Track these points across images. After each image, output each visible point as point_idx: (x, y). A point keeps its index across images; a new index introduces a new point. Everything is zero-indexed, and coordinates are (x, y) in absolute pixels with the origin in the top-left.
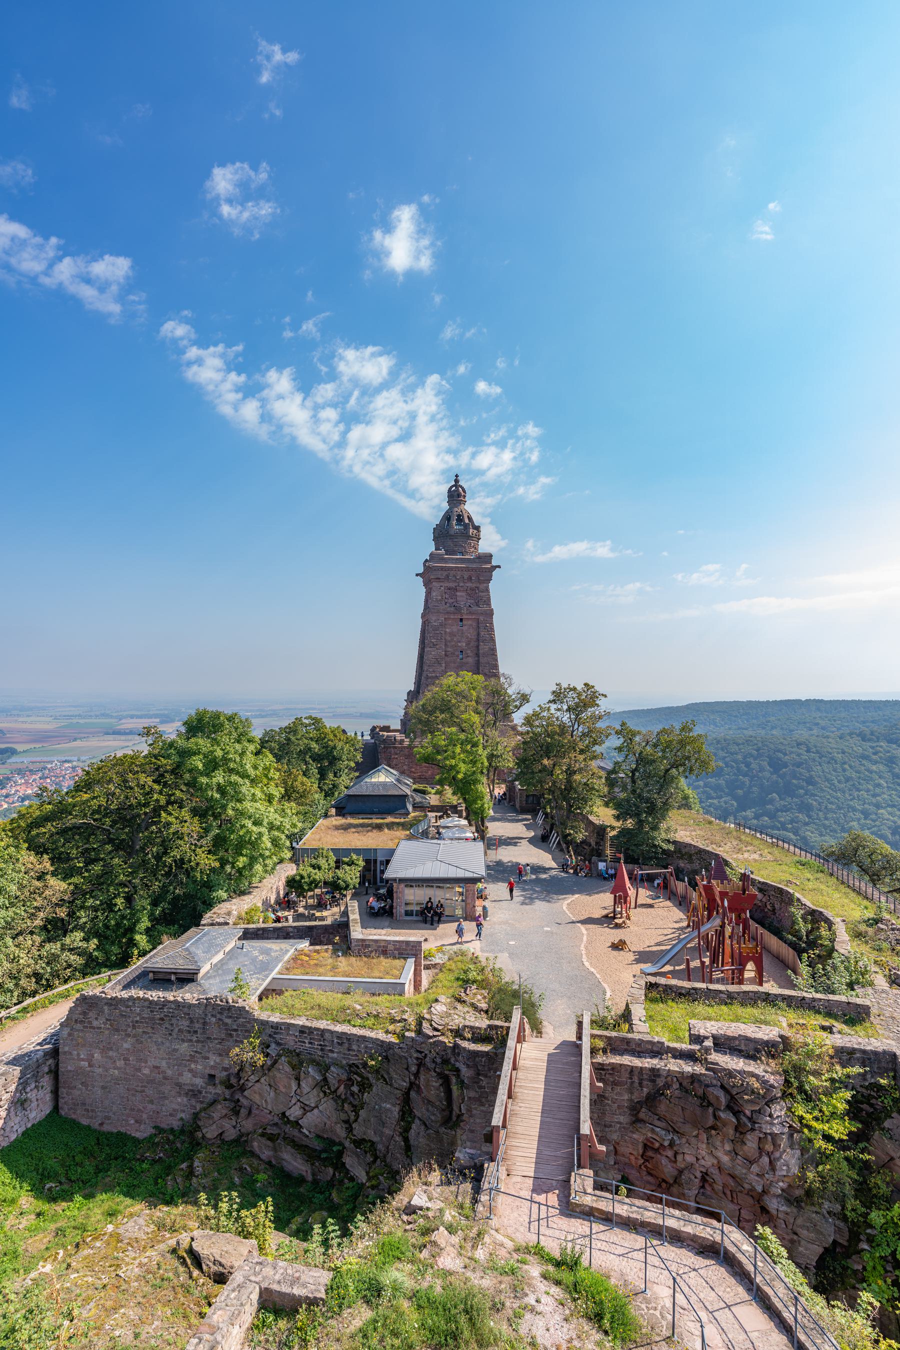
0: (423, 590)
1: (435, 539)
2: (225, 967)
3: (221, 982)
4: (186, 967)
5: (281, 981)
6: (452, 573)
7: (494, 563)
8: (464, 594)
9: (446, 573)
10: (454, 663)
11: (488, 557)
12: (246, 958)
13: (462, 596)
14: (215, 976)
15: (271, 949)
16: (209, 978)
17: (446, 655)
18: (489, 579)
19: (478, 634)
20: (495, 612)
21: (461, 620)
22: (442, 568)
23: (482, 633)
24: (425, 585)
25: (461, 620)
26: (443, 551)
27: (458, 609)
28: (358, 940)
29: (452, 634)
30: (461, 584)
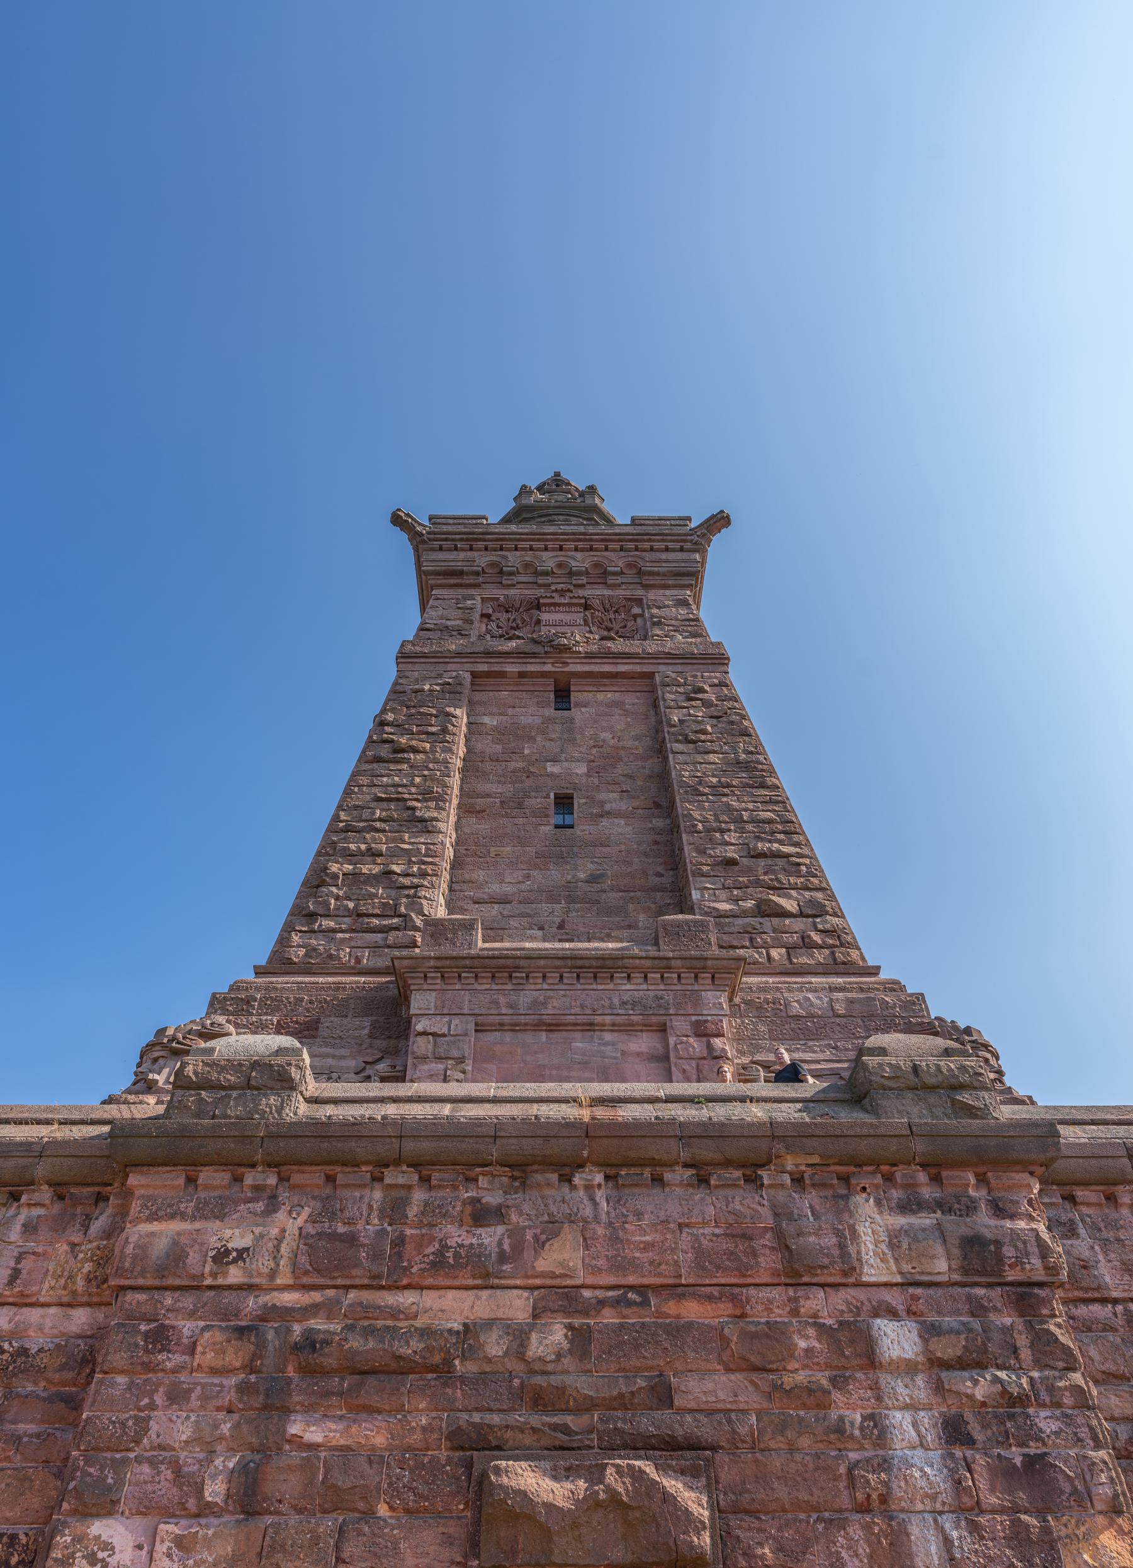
6: (513, 559)
9: (493, 557)
20: (730, 651)
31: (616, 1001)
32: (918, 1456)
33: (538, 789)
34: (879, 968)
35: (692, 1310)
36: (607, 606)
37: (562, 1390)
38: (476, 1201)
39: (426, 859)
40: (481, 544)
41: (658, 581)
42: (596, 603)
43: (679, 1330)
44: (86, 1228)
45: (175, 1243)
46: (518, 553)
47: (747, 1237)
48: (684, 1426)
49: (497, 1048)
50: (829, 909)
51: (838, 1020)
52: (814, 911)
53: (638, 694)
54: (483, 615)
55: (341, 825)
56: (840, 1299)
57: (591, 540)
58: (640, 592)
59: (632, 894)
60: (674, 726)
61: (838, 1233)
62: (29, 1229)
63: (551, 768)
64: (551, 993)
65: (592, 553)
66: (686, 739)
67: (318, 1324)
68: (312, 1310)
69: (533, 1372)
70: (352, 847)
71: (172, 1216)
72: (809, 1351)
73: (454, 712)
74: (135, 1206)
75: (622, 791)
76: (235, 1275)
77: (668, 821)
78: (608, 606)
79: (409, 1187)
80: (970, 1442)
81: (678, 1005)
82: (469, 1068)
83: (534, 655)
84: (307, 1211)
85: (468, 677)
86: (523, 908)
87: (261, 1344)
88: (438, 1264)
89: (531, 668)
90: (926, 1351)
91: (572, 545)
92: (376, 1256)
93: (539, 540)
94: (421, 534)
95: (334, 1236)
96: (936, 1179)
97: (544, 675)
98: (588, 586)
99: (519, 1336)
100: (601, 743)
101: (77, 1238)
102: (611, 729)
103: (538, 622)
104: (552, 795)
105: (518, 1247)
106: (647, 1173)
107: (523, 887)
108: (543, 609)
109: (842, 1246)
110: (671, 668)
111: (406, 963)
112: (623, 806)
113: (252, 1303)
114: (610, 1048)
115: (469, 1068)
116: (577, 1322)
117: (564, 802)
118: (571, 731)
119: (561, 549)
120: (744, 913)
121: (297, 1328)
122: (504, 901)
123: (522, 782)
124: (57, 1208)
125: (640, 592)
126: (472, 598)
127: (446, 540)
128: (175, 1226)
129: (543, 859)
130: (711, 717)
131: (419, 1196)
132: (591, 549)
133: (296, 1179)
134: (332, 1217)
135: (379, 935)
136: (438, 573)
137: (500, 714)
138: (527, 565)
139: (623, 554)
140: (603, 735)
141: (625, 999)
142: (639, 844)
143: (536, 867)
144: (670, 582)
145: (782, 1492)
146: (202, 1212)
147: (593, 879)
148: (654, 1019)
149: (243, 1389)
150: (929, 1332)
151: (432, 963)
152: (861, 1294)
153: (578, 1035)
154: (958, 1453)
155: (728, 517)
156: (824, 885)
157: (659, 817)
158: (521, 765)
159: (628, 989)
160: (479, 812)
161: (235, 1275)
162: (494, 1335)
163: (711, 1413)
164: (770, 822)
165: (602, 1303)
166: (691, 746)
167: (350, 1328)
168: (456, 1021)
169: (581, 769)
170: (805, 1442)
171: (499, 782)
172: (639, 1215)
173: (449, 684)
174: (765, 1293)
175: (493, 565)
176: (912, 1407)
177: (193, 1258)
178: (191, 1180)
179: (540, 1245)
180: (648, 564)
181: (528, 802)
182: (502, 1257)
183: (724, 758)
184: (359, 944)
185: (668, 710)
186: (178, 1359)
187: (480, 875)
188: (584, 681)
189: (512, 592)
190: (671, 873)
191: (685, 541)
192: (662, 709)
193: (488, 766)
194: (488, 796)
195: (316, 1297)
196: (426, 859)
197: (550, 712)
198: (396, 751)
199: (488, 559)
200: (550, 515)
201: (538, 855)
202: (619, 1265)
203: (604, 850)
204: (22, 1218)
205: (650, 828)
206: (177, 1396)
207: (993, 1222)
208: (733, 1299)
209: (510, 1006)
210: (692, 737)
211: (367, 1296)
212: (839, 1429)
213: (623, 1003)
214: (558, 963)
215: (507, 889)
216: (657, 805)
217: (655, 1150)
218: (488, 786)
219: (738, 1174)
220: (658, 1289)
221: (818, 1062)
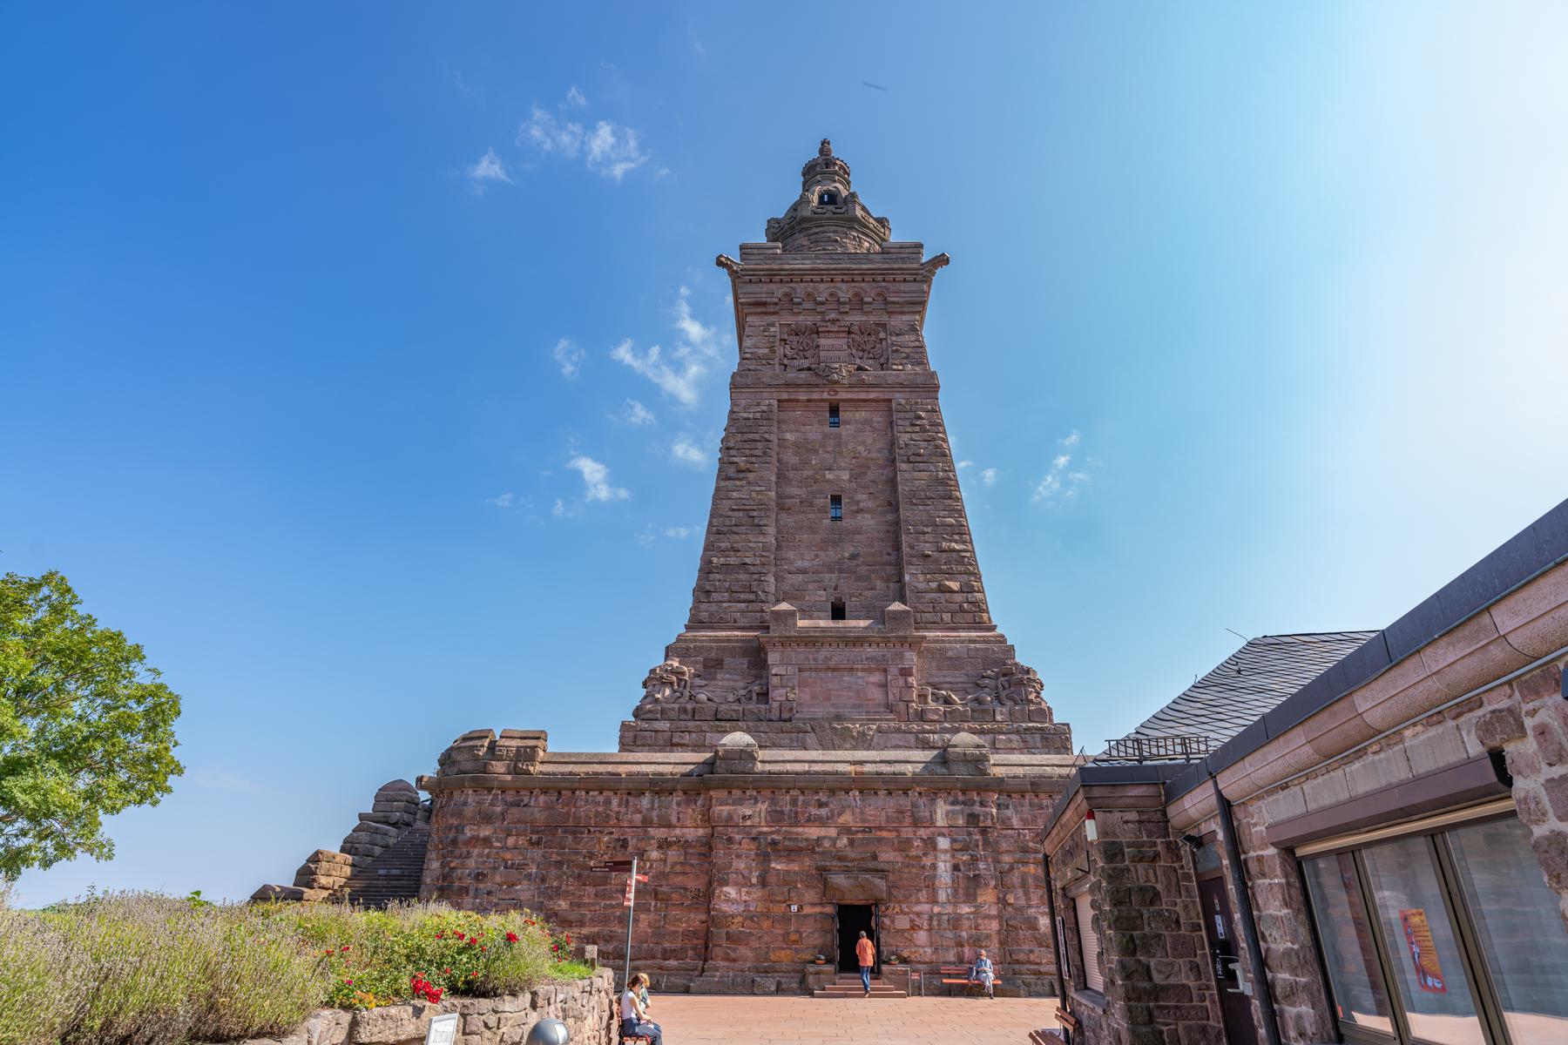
6: (800, 290)
8: (842, 342)
9: (785, 289)
10: (813, 531)
13: (831, 349)
18: (919, 305)
19: (892, 444)
20: (942, 381)
21: (834, 410)
23: (904, 438)
25: (834, 410)
27: (821, 376)
29: (803, 447)
31: (864, 657)
32: (944, 875)
33: (821, 492)
34: (996, 626)
35: (884, 834)
36: (863, 330)
37: (846, 856)
38: (819, 800)
39: (764, 554)
40: (777, 278)
41: (897, 308)
42: (855, 329)
43: (880, 840)
44: (696, 804)
45: (729, 813)
46: (803, 285)
47: (902, 812)
48: (881, 866)
49: (809, 680)
50: (976, 589)
51: (970, 660)
52: (968, 589)
53: (881, 413)
54: (781, 340)
55: (715, 529)
56: (928, 831)
57: (853, 274)
58: (885, 318)
59: (874, 567)
60: (902, 448)
61: (931, 812)
62: (678, 804)
63: (829, 476)
64: (833, 653)
65: (854, 284)
66: (908, 459)
67: (774, 837)
68: (773, 833)
69: (838, 851)
70: (723, 545)
71: (727, 805)
72: (917, 846)
73: (770, 438)
74: (714, 801)
75: (870, 493)
76: (748, 823)
77: (895, 516)
78: (866, 331)
79: (798, 796)
80: (960, 870)
81: (893, 660)
82: (797, 692)
83: (817, 386)
84: (767, 803)
85: (775, 403)
86: (816, 577)
87: (760, 843)
88: (809, 820)
89: (815, 396)
90: (951, 847)
91: (839, 278)
92: (790, 818)
93: (817, 275)
94: (736, 272)
95: (777, 811)
96: (964, 794)
97: (822, 400)
98: (851, 312)
99: (834, 841)
100: (858, 455)
101: (694, 807)
102: (864, 443)
103: (818, 346)
104: (829, 497)
105: (833, 815)
106: (872, 792)
107: (815, 563)
109: (931, 816)
110: (902, 395)
111: (765, 639)
112: (870, 504)
113: (754, 831)
114: (860, 680)
115: (797, 692)
116: (850, 837)
117: (836, 500)
118: (839, 445)
119: (832, 281)
120: (932, 591)
121: (769, 838)
122: (804, 571)
124: (684, 797)
125: (885, 318)
126: (774, 326)
127: (754, 275)
128: (728, 808)
129: (824, 545)
130: (925, 441)
131: (801, 798)
132: (853, 281)
133: (762, 793)
134: (775, 806)
135: (744, 604)
137: (797, 431)
138: (809, 295)
139: (874, 285)
140: (861, 448)
141: (868, 656)
142: (879, 532)
143: (821, 549)
144: (906, 310)
145: (905, 882)
146: (734, 804)
147: (854, 557)
148: (881, 666)
149: (756, 854)
150: (954, 841)
151: (777, 639)
152: (935, 829)
153: (846, 673)
154: (956, 873)
155: (948, 259)
156: (976, 571)
157: (892, 513)
158: (811, 473)
159: (870, 651)
160: (789, 509)
161: (748, 823)
162: (827, 840)
163: (888, 862)
164: (952, 525)
165: (858, 832)
166: (911, 465)
167: (784, 838)
168: (790, 668)
169: (846, 476)
170: (914, 870)
171: (798, 487)
172: (870, 805)
173: (765, 412)
174: (906, 829)
175: (786, 295)
176: (946, 861)
177: (735, 818)
178: (730, 793)
179: (839, 815)
181: (817, 501)
182: (828, 818)
183: (930, 475)
184: (734, 609)
185: (899, 434)
186: (736, 846)
187: (791, 555)
188: (846, 404)
189: (800, 318)
190: (896, 553)
191: (916, 274)
192: (895, 433)
193: (791, 474)
194: (793, 497)
195: (773, 829)
196: (764, 554)
197: (827, 429)
198: (740, 471)
199: (783, 290)
200: (823, 226)
201: (823, 541)
202: (863, 821)
203: (860, 537)
204: (675, 801)
205: (886, 522)
206: (738, 856)
207: (979, 808)
208: (897, 831)
209: (815, 660)
210: (912, 459)
211: (788, 829)
212: (923, 867)
213: (868, 658)
214: (837, 639)
215: (806, 564)
216: (890, 504)
217: (876, 786)
218: (792, 489)
219: (901, 792)
220: (875, 827)
221: (957, 683)
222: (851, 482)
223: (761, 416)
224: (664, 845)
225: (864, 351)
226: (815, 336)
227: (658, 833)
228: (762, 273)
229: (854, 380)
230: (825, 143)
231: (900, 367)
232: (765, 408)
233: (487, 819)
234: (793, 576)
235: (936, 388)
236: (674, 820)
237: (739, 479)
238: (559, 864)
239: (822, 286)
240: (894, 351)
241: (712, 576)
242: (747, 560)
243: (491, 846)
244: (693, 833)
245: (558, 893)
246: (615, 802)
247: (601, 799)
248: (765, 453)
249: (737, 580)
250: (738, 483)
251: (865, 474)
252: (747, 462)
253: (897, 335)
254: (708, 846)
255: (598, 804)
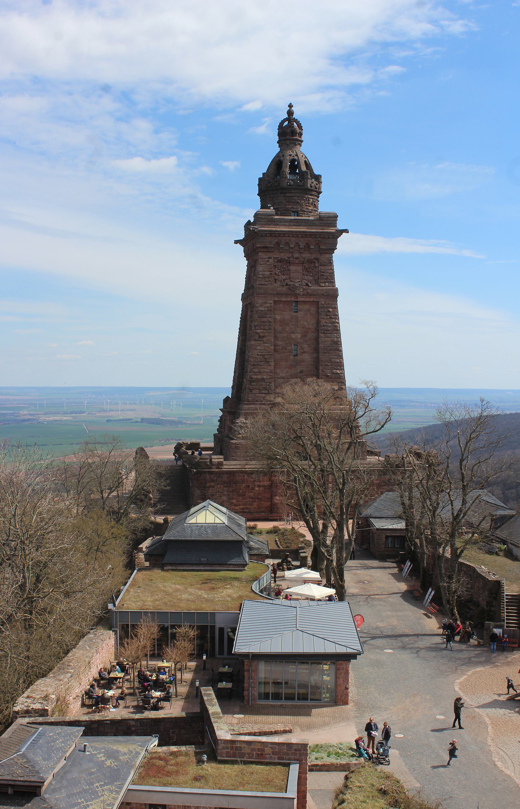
0: (244, 263)
1: (261, 193)
2: (69, 776)
3: (69, 796)
4: (26, 779)
5: (138, 793)
7: (340, 226)
8: (300, 268)
9: (276, 240)
11: (332, 219)
12: (91, 764)
14: (60, 789)
15: (118, 752)
16: (54, 791)
17: (275, 350)
18: (333, 248)
19: (318, 322)
22: (271, 234)
24: (247, 255)
26: (271, 210)
28: (226, 741)
30: (296, 255)
55: (252, 363)
63: (293, 336)
73: (271, 321)
78: (310, 261)
108: (291, 264)
122: (283, 378)
123: (286, 341)
136: (260, 247)
140: (306, 323)
147: (301, 372)
169: (299, 336)
180: (322, 245)
184: (261, 397)
189: (282, 254)
194: (279, 346)
199: (276, 241)
203: (303, 363)
216: (315, 349)
222: (301, 339)
223: (267, 309)
224: (259, 486)
225: (308, 272)
226: (288, 264)
227: (257, 483)
228: (267, 232)
229: (305, 292)
230: (290, 106)
231: (324, 285)
232: (269, 305)
233: (213, 481)
234: (279, 380)
235: (337, 296)
236: (262, 480)
237: (260, 341)
238: (232, 491)
239: (293, 239)
240: (322, 275)
241: (252, 384)
242: (265, 377)
243: (214, 487)
244: (267, 483)
245: (233, 499)
246: (246, 476)
247: (242, 475)
248: (269, 328)
249: (261, 385)
250: (260, 342)
251: (307, 335)
252: (263, 332)
253: (323, 265)
254: (270, 487)
255: (241, 476)
